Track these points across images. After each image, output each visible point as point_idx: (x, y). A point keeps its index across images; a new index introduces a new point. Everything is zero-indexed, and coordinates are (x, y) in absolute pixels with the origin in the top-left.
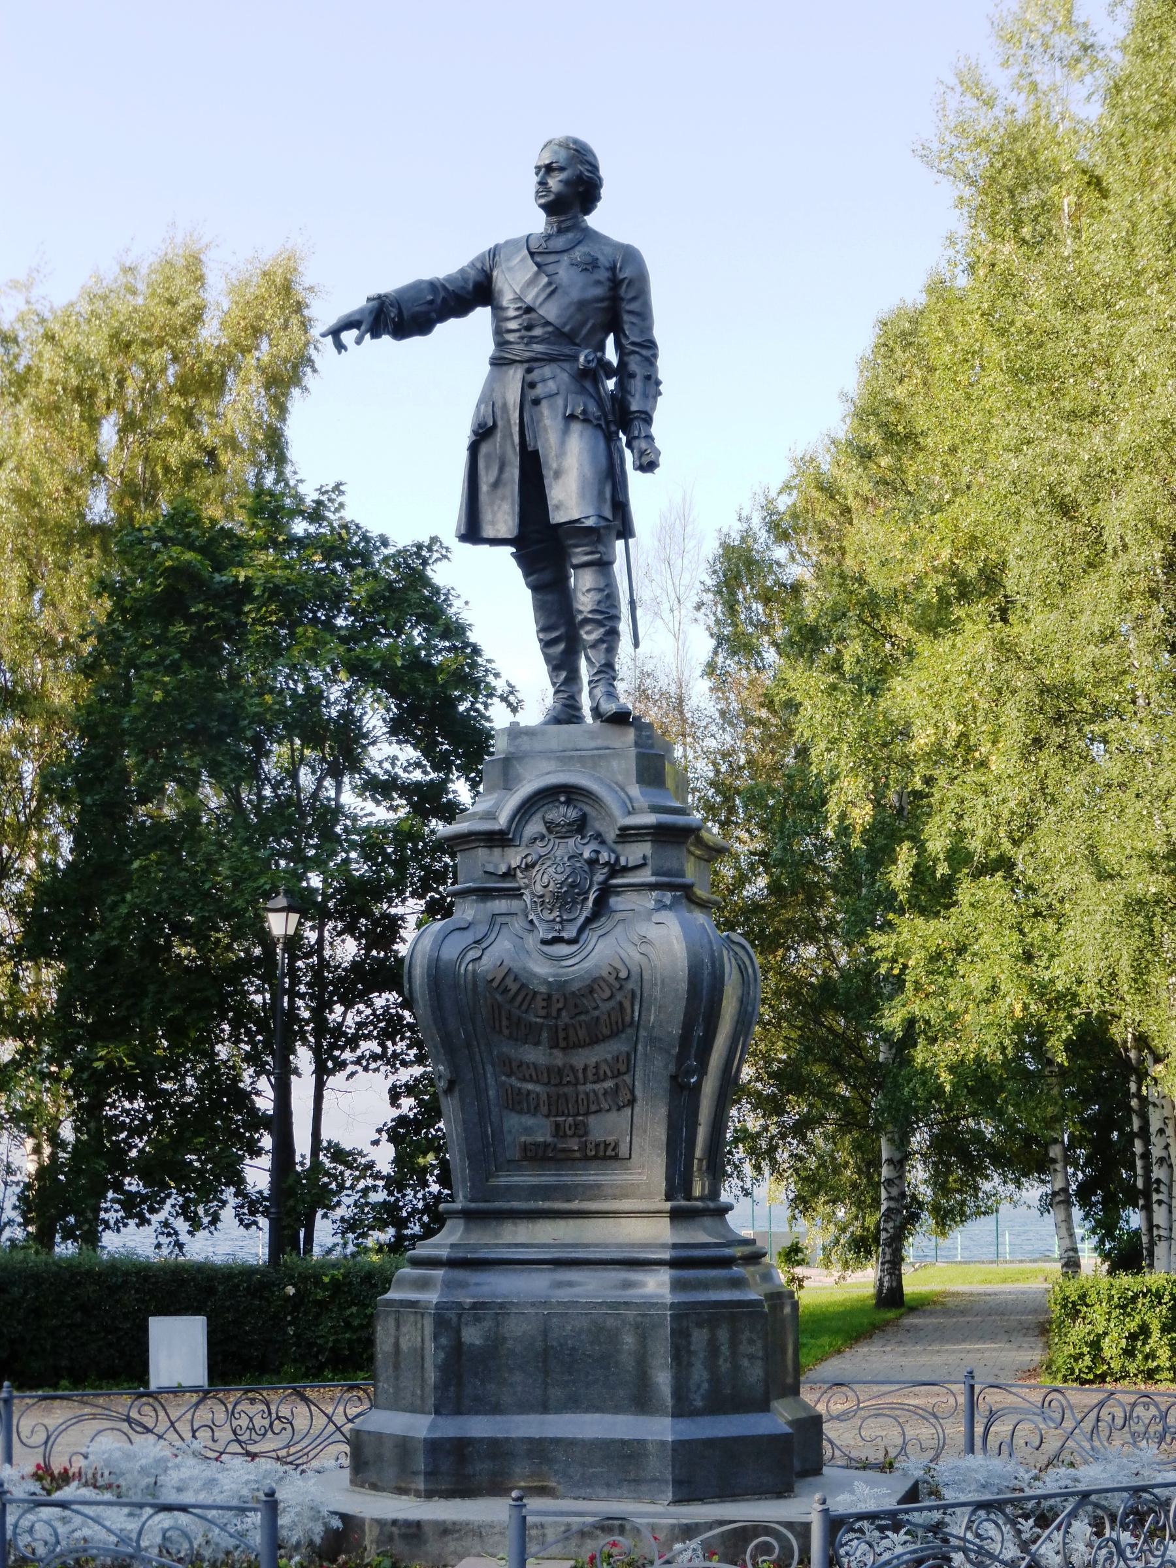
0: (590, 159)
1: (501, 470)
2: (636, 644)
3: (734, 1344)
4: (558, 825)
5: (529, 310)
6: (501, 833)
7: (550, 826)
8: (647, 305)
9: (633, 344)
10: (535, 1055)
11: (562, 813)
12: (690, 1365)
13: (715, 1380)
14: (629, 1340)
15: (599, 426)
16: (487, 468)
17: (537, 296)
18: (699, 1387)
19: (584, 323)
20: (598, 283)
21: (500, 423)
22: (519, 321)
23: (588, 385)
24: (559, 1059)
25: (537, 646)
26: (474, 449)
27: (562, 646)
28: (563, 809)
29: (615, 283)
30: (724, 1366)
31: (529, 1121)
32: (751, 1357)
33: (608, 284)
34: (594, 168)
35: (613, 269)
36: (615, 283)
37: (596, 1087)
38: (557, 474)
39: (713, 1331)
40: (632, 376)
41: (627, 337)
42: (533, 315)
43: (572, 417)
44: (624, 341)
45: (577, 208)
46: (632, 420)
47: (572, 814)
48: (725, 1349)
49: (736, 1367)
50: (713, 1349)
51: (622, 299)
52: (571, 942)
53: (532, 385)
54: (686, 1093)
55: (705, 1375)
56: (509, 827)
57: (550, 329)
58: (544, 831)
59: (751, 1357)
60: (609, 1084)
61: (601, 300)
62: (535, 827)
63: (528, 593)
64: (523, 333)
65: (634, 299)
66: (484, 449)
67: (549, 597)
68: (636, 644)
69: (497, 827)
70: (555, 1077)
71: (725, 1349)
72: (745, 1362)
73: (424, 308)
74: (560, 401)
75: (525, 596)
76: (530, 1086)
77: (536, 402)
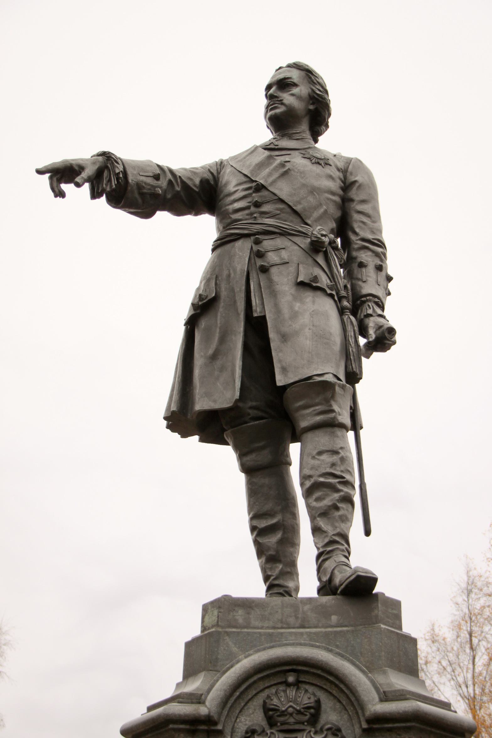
0: (320, 81)
1: (223, 340)
2: (368, 532)
4: (283, 713)
5: (260, 188)
6: (209, 720)
7: (272, 716)
8: (376, 209)
9: (363, 240)
11: (288, 699)
15: (331, 296)
16: (207, 339)
17: (270, 175)
19: (316, 208)
20: (331, 177)
21: (224, 294)
22: (249, 200)
23: (320, 259)
25: (247, 538)
26: (192, 324)
27: (279, 535)
28: (292, 692)
29: (347, 186)
33: (339, 183)
34: (326, 92)
35: (345, 172)
36: (347, 186)
38: (284, 338)
40: (362, 265)
41: (356, 233)
42: (264, 193)
43: (302, 284)
44: (353, 237)
45: (304, 127)
46: (364, 302)
47: (305, 698)
51: (352, 200)
53: (260, 255)
56: (220, 714)
57: (281, 206)
58: (264, 723)
61: (333, 193)
62: (252, 717)
63: (241, 478)
64: (253, 209)
65: (363, 202)
66: (203, 323)
67: (266, 481)
68: (368, 532)
69: (203, 710)
73: (150, 181)
74: (292, 269)
75: (239, 480)
77: (264, 270)
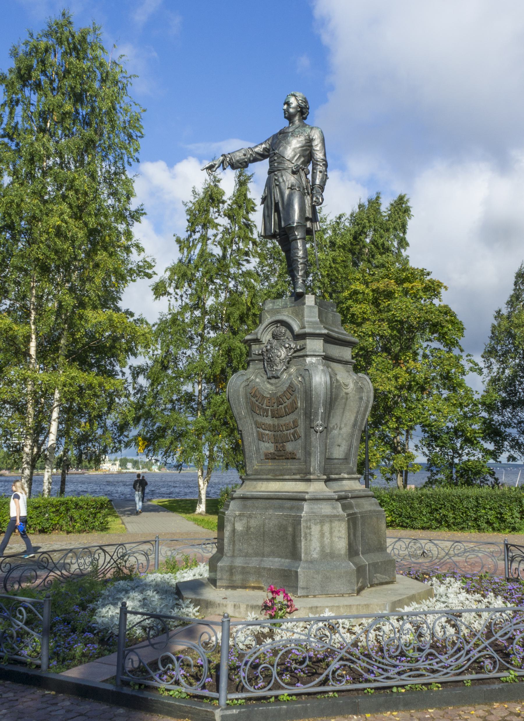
3: (331, 533)
10: (269, 421)
12: (311, 540)
13: (322, 547)
14: (290, 529)
18: (315, 549)
24: (276, 421)
30: (327, 541)
31: (266, 444)
32: (340, 537)
37: (288, 432)
39: (322, 527)
48: (327, 534)
49: (332, 542)
50: (322, 535)
52: (278, 378)
54: (319, 433)
55: (318, 544)
59: (340, 537)
60: (292, 431)
70: (274, 428)
71: (327, 534)
72: (337, 540)
76: (267, 432)
